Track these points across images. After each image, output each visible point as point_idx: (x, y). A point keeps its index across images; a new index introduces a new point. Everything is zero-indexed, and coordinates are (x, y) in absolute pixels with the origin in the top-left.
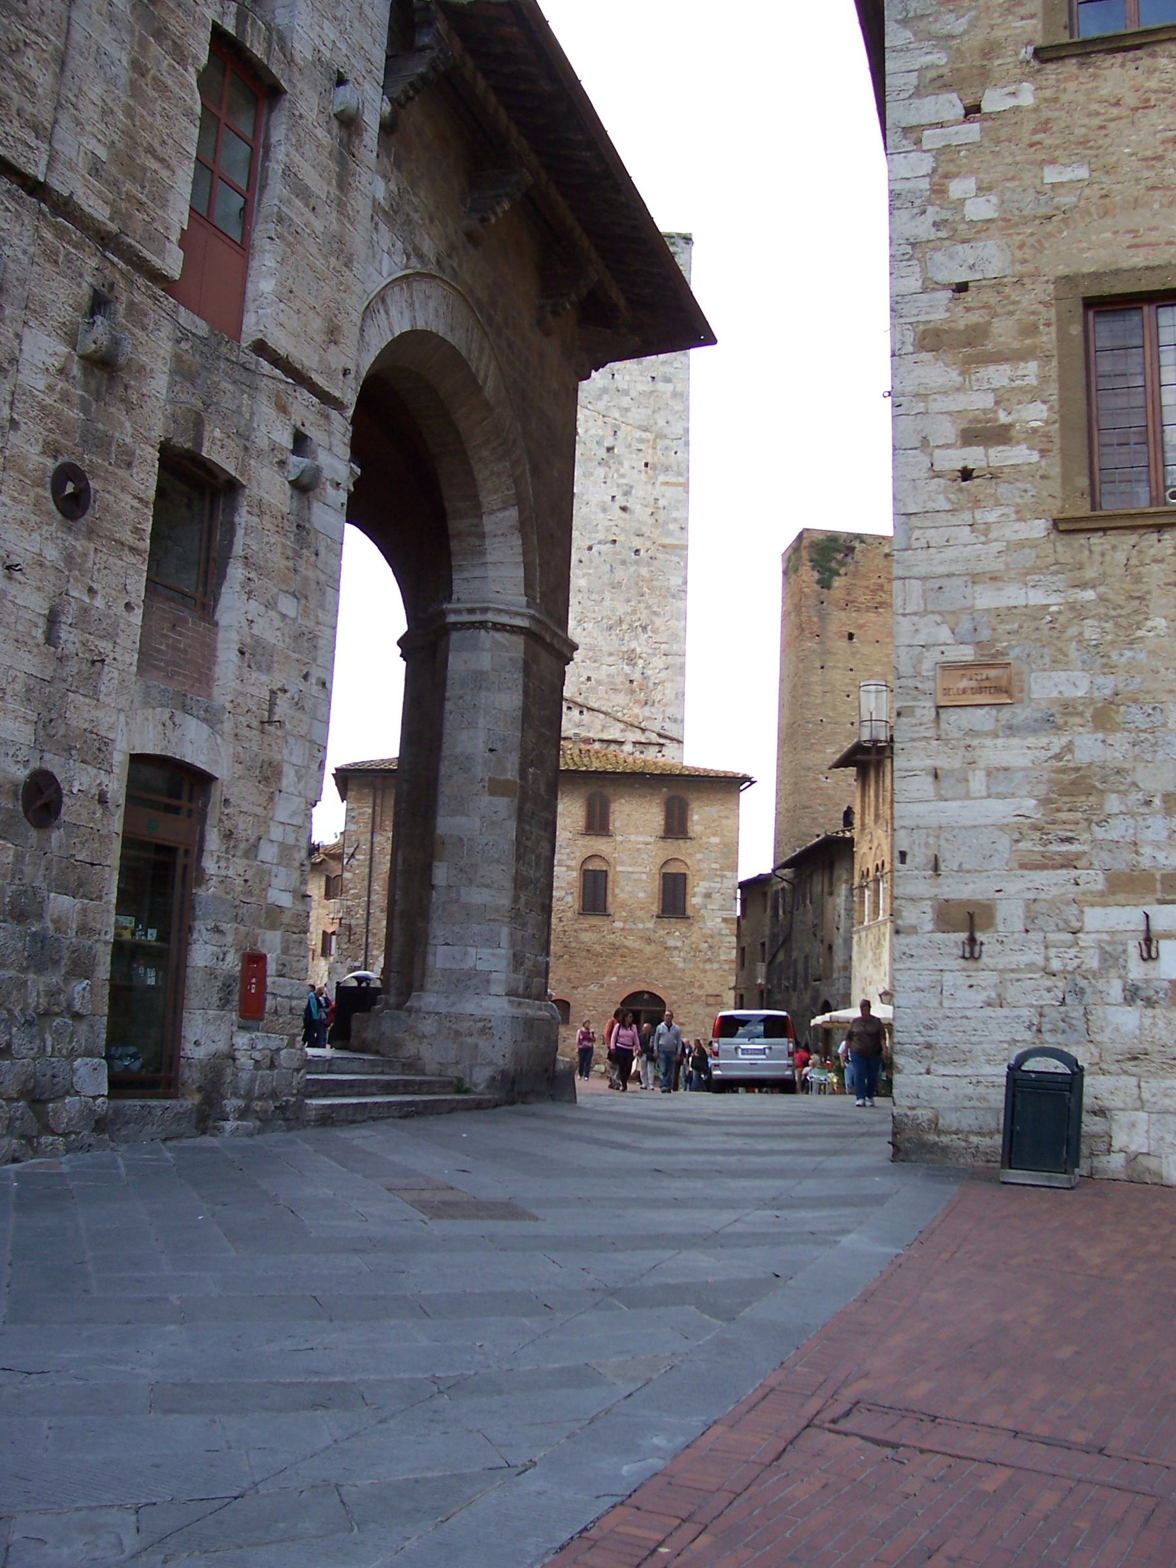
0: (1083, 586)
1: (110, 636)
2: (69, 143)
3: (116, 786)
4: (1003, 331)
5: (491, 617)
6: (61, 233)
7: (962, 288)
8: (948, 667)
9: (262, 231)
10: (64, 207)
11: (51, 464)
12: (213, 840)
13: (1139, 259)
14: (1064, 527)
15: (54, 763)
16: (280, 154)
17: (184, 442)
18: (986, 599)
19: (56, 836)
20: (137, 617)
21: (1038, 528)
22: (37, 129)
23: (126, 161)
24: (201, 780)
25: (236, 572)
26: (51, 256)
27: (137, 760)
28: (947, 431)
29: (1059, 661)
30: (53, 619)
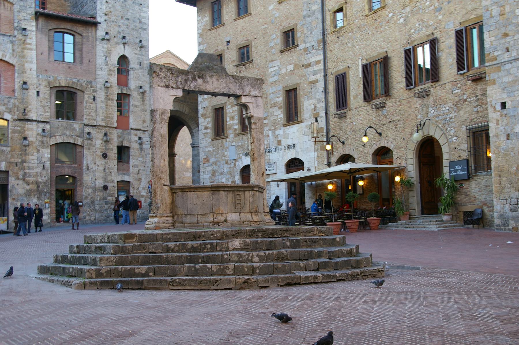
0: (214, 147)
1: (113, 169)
2: (99, 119)
3: (116, 185)
4: (208, 115)
5: (196, 145)
6: (99, 129)
7: (204, 108)
8: (204, 158)
9: (130, 113)
10: (100, 126)
11: (102, 154)
12: (131, 189)
13: (218, 103)
14: (213, 140)
15: (106, 184)
16: (131, 103)
17: (120, 145)
18: (207, 149)
19: (108, 191)
20: (116, 166)
21: (210, 140)
22: (94, 120)
23: (107, 117)
24: (129, 182)
25: (131, 157)
26: (98, 132)
27: (118, 182)
28: (203, 128)
29: (212, 157)
30: (104, 169)
